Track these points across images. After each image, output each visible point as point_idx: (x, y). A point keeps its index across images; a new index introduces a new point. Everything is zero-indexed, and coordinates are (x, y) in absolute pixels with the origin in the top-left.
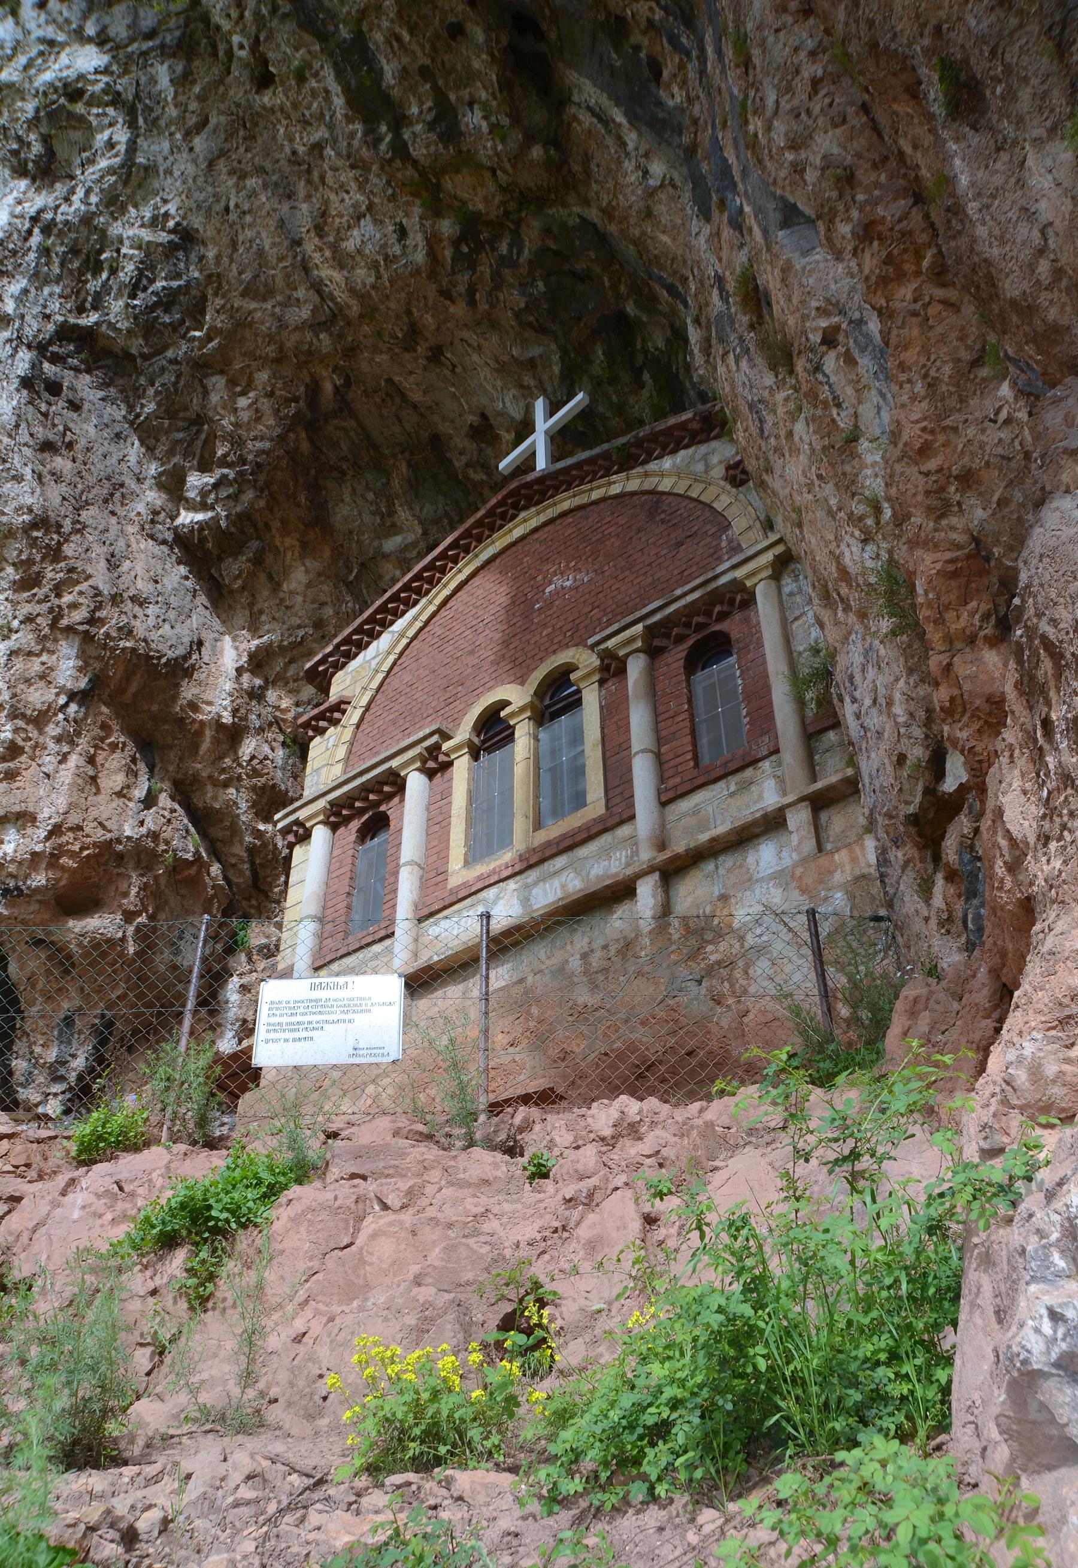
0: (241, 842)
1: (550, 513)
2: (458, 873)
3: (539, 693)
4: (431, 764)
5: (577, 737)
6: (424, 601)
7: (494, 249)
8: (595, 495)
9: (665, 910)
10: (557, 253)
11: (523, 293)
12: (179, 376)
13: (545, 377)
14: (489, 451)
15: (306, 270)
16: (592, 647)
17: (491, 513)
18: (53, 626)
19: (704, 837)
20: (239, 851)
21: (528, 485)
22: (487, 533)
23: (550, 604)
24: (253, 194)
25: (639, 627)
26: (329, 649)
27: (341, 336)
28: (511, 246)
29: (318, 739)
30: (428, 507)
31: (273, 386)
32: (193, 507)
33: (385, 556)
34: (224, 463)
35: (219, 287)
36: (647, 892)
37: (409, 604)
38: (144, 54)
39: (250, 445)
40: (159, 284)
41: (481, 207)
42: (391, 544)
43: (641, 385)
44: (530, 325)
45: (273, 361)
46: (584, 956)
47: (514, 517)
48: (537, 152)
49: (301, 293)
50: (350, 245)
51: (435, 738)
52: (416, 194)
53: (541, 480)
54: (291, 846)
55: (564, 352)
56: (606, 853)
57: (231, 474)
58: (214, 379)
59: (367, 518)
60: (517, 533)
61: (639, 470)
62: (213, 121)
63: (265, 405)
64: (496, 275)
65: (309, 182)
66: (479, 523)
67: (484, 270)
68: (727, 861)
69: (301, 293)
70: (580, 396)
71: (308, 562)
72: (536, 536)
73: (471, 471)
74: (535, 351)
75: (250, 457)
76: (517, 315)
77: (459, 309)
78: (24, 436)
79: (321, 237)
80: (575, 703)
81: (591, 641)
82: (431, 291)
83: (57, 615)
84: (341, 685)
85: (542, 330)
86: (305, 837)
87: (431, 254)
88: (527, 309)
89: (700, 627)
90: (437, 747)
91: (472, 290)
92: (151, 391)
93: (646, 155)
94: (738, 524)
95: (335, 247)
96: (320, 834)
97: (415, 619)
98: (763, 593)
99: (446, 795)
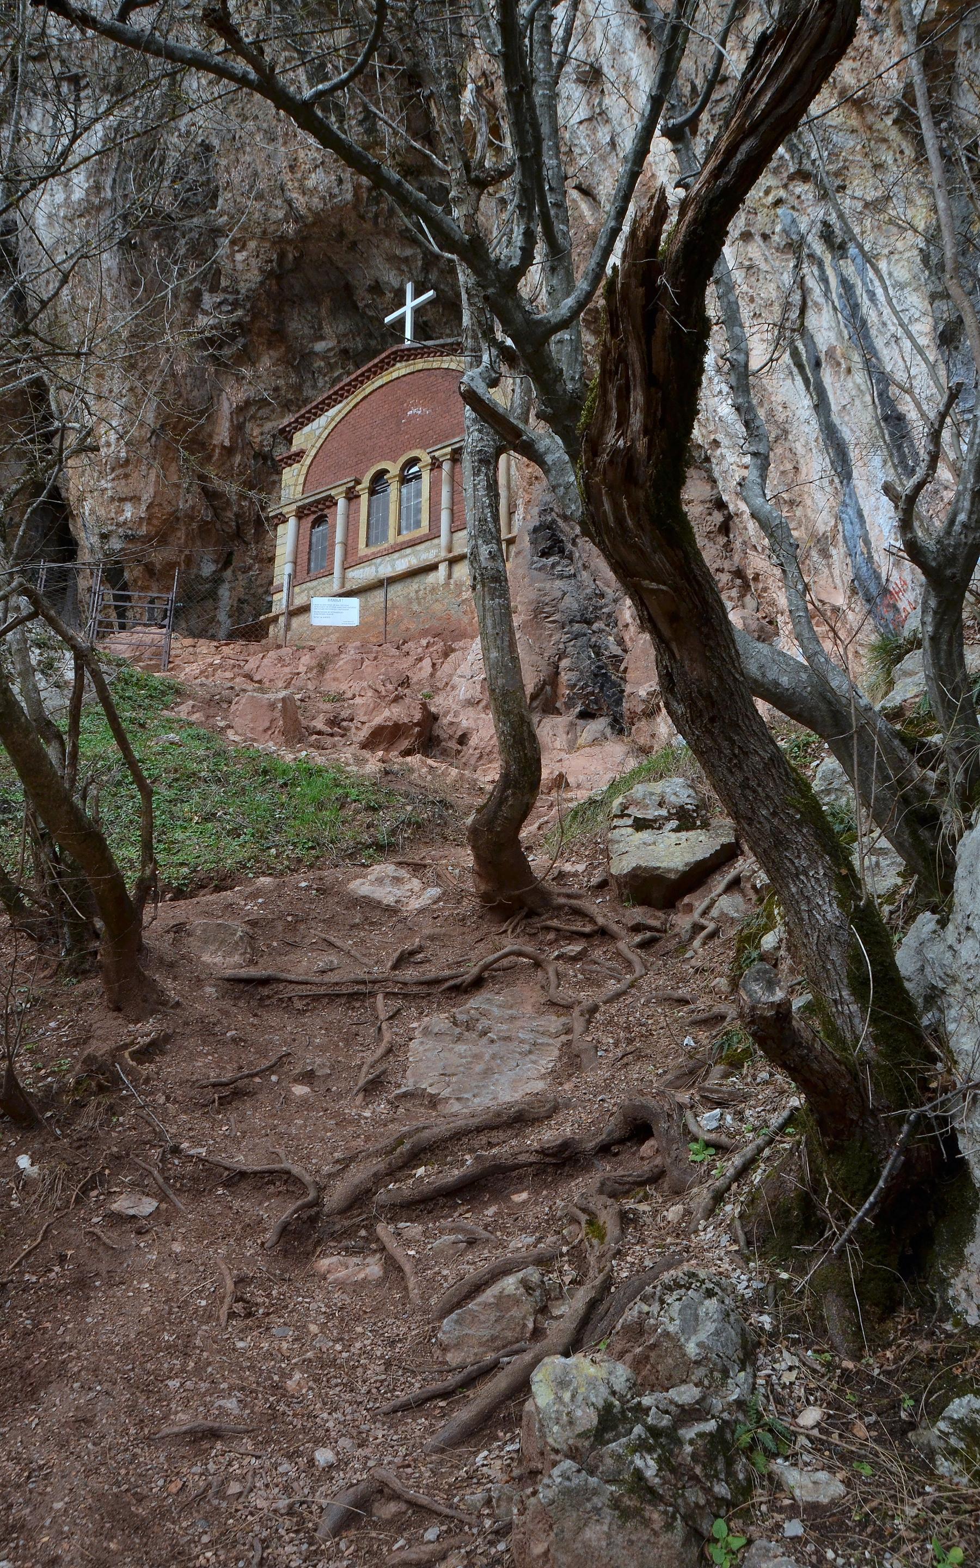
0: (231, 510)
2: (362, 550)
3: (402, 469)
5: (418, 494)
6: (345, 402)
8: (435, 365)
9: (450, 576)
12: (200, 235)
15: (283, 190)
17: (382, 361)
20: (230, 514)
21: (402, 351)
23: (409, 422)
24: (251, 135)
25: (449, 449)
29: (288, 469)
30: (341, 327)
32: (206, 313)
33: (316, 354)
34: (225, 290)
36: (443, 568)
37: (337, 402)
39: (242, 284)
42: (320, 346)
46: (417, 592)
50: (310, 183)
51: (352, 484)
53: (409, 350)
54: (277, 525)
56: (427, 550)
57: (231, 298)
59: (306, 331)
60: (395, 375)
63: (253, 262)
66: (375, 366)
69: (279, 202)
70: (431, 293)
71: (271, 352)
73: (367, 310)
75: (243, 291)
77: (368, 226)
78: (124, 282)
79: (293, 173)
80: (418, 477)
82: (353, 215)
84: (299, 440)
86: (285, 521)
90: (354, 487)
91: (376, 216)
96: (292, 521)
99: (358, 511)
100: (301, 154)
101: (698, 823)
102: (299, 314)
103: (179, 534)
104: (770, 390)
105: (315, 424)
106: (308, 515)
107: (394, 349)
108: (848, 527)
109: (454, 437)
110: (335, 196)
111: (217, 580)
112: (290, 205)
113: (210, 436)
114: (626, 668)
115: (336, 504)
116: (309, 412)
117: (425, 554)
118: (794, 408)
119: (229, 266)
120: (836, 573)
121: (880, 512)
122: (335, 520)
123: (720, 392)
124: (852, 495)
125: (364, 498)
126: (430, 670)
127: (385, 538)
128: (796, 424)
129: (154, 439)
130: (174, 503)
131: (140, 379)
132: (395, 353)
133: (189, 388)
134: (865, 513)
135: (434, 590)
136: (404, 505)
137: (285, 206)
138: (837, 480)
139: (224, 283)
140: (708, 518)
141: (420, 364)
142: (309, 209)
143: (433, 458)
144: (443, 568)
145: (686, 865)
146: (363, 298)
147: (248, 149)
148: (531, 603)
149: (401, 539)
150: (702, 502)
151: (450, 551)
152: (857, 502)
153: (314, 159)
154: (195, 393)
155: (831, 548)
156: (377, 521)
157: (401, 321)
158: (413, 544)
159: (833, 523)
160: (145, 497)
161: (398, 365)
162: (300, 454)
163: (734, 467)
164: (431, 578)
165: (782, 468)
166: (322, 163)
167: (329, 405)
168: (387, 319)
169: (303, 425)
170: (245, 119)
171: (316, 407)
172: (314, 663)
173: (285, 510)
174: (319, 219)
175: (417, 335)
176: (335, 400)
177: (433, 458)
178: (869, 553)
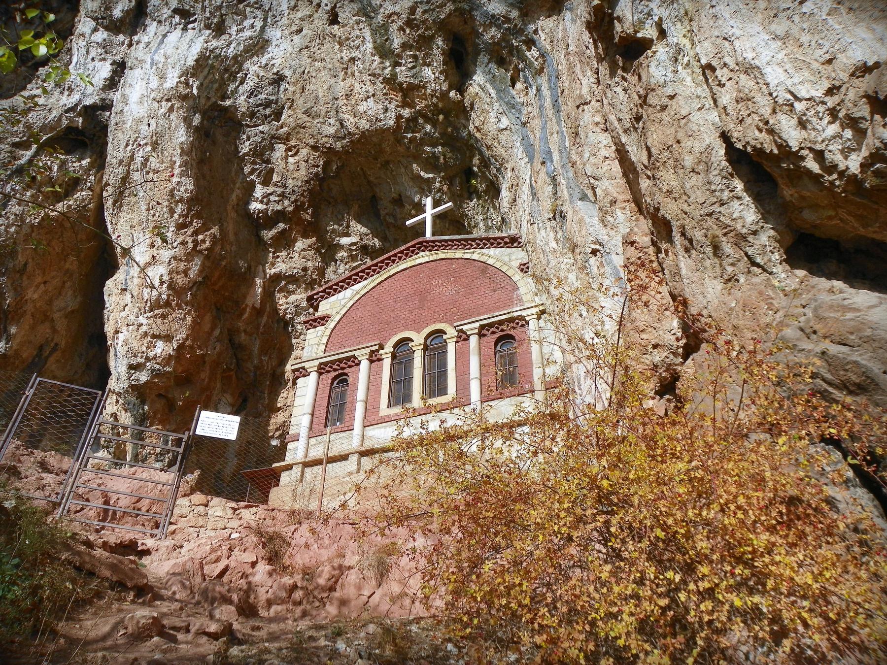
1: (435, 257)
3: (426, 339)
4: (374, 358)
14: (398, 210)
16: (455, 327)
22: (404, 257)
34: (275, 185)
35: (292, 106)
39: (291, 181)
40: (262, 96)
42: (345, 241)
44: (431, 163)
45: (311, 147)
47: (418, 253)
49: (332, 121)
51: (376, 347)
57: (279, 190)
63: (303, 165)
69: (332, 121)
70: (450, 204)
72: (427, 265)
75: (290, 186)
81: (455, 324)
82: (392, 138)
83: (196, 243)
90: (377, 351)
92: (248, 143)
95: (353, 107)
96: (314, 376)
97: (365, 287)
99: (380, 373)
100: (357, 86)
102: (333, 213)
105: (341, 295)
113: (245, 297)
115: (358, 364)
129: (194, 289)
131: (192, 235)
139: (275, 178)
142: (357, 128)
146: (385, 207)
157: (423, 223)
161: (422, 253)
162: (324, 319)
166: (373, 95)
167: (355, 280)
175: (434, 234)
176: (361, 277)
177: (462, 331)
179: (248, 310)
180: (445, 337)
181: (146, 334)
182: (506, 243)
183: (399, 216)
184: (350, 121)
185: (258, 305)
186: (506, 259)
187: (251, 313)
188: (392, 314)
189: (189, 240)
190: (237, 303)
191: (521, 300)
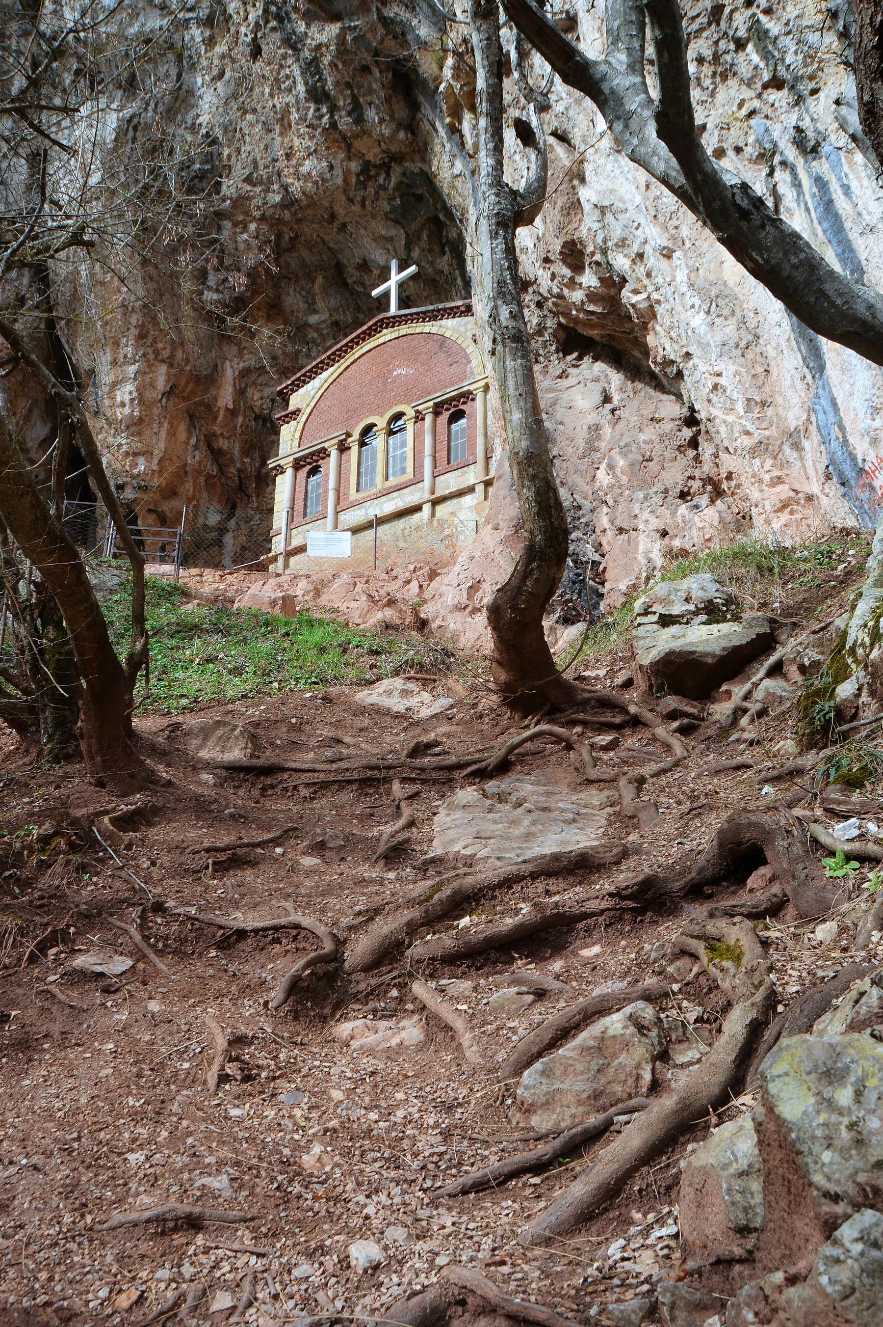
2: (353, 495)
5: (403, 444)
6: (336, 365)
7: (376, 180)
8: (418, 330)
10: (407, 185)
11: (389, 204)
13: (397, 246)
15: (279, 176)
17: (370, 328)
18: (156, 359)
19: (447, 492)
21: (388, 318)
23: (394, 381)
26: (289, 382)
27: (295, 213)
28: (385, 179)
31: (258, 233)
32: (209, 288)
33: (310, 326)
36: (427, 508)
38: (187, 21)
41: (371, 158)
42: (313, 319)
43: (444, 254)
48: (402, 135)
49: (276, 187)
50: (304, 169)
51: (344, 437)
52: (340, 147)
53: (394, 317)
54: (276, 475)
55: (407, 235)
56: (412, 493)
58: (225, 222)
60: (381, 340)
61: (438, 323)
62: (228, 75)
64: (377, 193)
65: (282, 125)
66: (364, 332)
67: (371, 190)
68: (455, 501)
69: (276, 187)
74: (393, 233)
76: (386, 214)
77: (356, 208)
82: (343, 198)
83: (157, 353)
84: (295, 401)
85: (397, 222)
87: (346, 180)
88: (391, 212)
89: (455, 406)
90: (345, 440)
91: (364, 200)
93: (454, 156)
94: (474, 363)
96: (289, 472)
98: (479, 397)
99: (348, 461)
100: (296, 142)
101: (729, 616)
103: (187, 486)
104: (742, 298)
106: (304, 466)
107: (381, 316)
108: (821, 416)
109: (435, 392)
110: (327, 181)
111: (222, 530)
112: (286, 190)
113: (215, 399)
114: (605, 568)
115: (329, 456)
116: (304, 375)
117: (409, 498)
118: (765, 313)
119: (231, 247)
120: (809, 463)
121: (855, 397)
122: (328, 469)
123: (693, 306)
124: (826, 386)
125: (355, 449)
126: (417, 590)
127: (372, 483)
128: (767, 327)
129: (164, 400)
130: (183, 458)
131: (152, 346)
132: (381, 320)
133: (196, 355)
134: (839, 401)
135: (418, 528)
136: (391, 454)
137: (282, 191)
138: (809, 377)
140: (678, 433)
141: (404, 330)
143: (417, 412)
144: (427, 508)
145: (724, 649)
146: (352, 275)
147: (248, 139)
148: (512, 519)
149: (388, 484)
150: (672, 420)
151: (433, 493)
152: (830, 391)
153: (308, 148)
154: (202, 360)
155: (803, 440)
156: (366, 469)
157: (386, 295)
158: (399, 488)
159: (805, 417)
160: (156, 452)
161: (385, 331)
162: (297, 412)
163: (707, 375)
164: (416, 516)
165: (753, 372)
166: (315, 151)
167: (322, 369)
168: (374, 293)
169: (299, 387)
170: (245, 112)
171: (310, 371)
172: (311, 587)
173: (282, 462)
174: (312, 201)
176: (328, 364)
177: (417, 412)
178: (844, 437)
179: (221, 412)
180: (404, 418)
181: (127, 454)
182: (462, 312)
183: (368, 283)
184: (296, 187)
185: (231, 406)
186: (462, 329)
187: (225, 415)
188: (358, 400)
189: (150, 350)
190: (208, 407)
191: (472, 373)
